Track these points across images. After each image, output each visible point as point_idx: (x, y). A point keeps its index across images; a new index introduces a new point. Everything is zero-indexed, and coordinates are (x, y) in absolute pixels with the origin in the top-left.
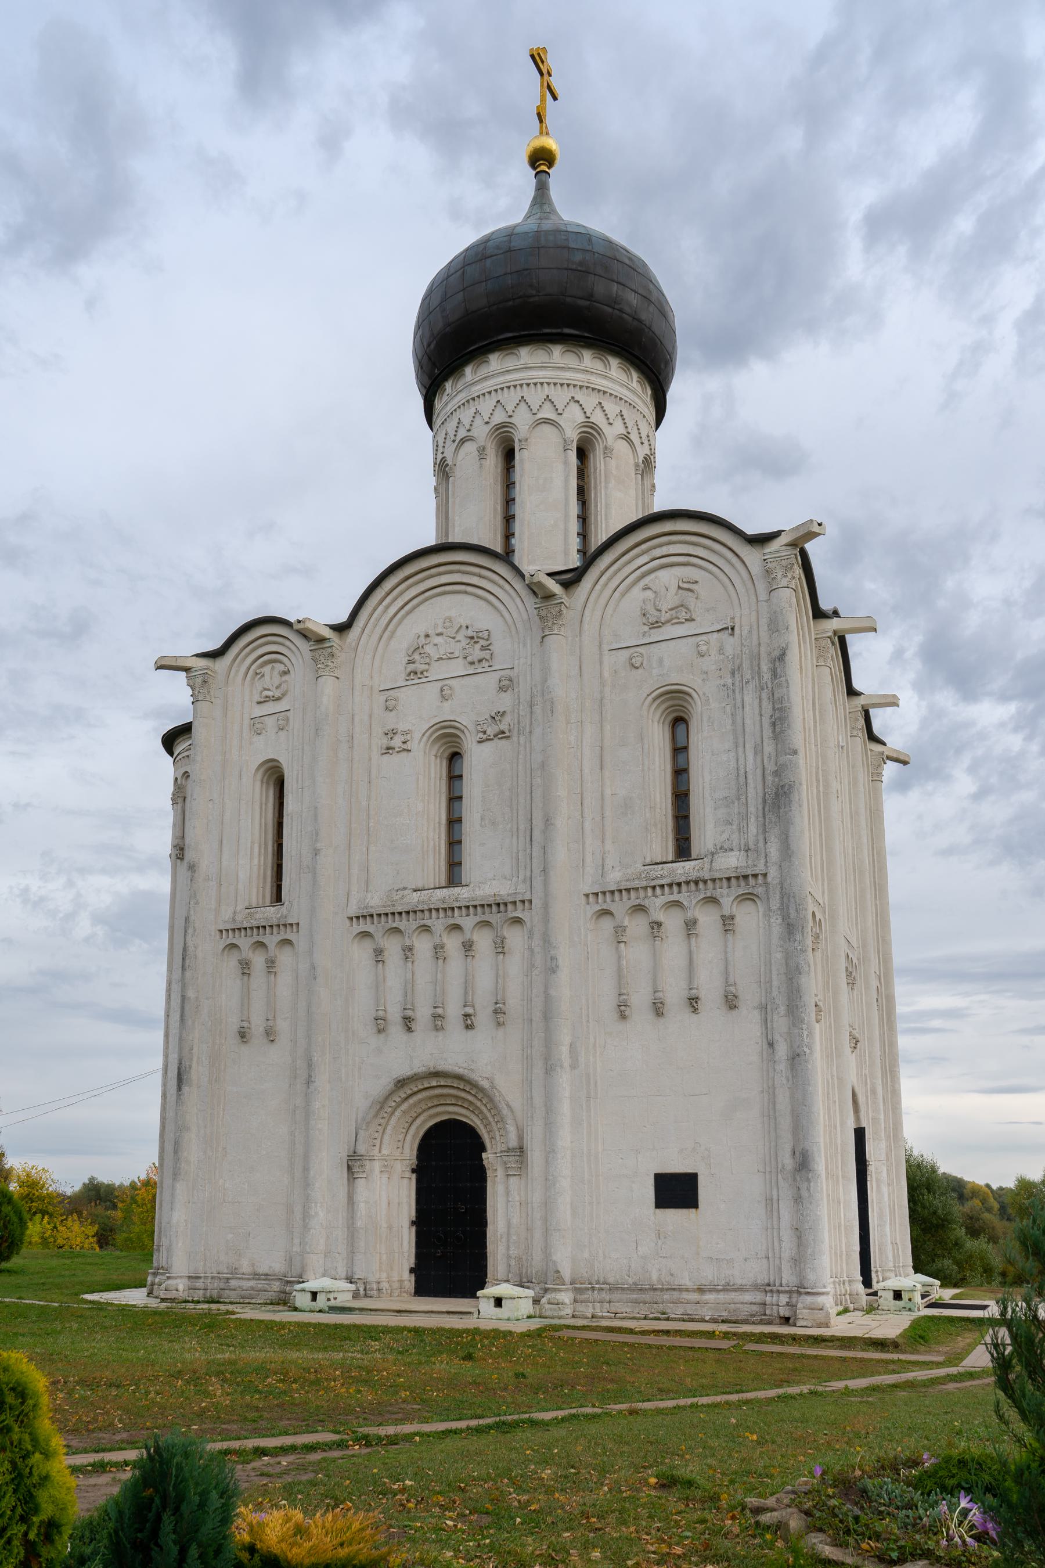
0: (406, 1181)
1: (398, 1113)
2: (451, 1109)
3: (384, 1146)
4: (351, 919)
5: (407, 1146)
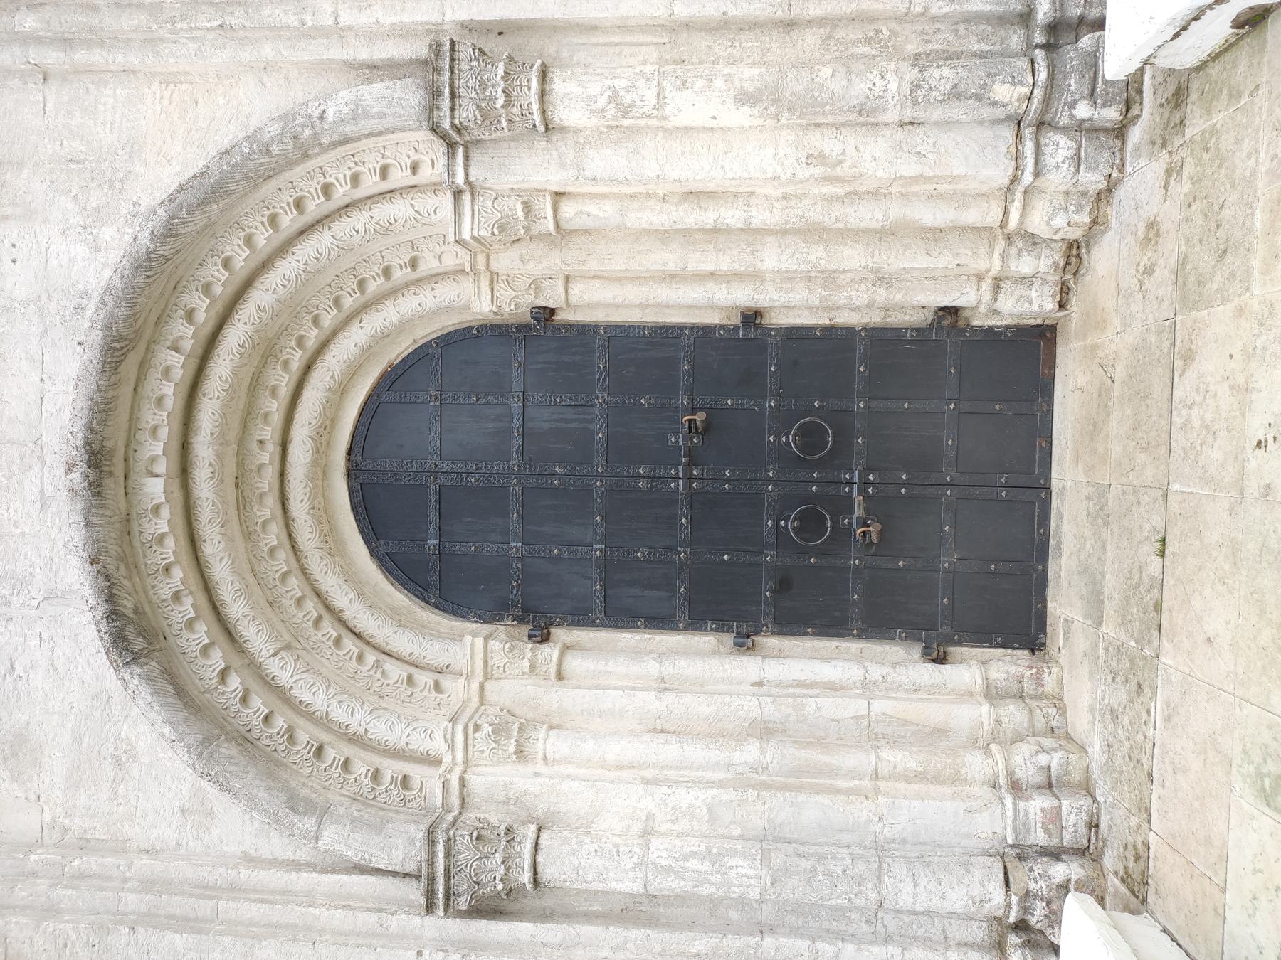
0: (575, 664)
1: (282, 671)
2: (300, 454)
3: (418, 743)
5: (435, 652)
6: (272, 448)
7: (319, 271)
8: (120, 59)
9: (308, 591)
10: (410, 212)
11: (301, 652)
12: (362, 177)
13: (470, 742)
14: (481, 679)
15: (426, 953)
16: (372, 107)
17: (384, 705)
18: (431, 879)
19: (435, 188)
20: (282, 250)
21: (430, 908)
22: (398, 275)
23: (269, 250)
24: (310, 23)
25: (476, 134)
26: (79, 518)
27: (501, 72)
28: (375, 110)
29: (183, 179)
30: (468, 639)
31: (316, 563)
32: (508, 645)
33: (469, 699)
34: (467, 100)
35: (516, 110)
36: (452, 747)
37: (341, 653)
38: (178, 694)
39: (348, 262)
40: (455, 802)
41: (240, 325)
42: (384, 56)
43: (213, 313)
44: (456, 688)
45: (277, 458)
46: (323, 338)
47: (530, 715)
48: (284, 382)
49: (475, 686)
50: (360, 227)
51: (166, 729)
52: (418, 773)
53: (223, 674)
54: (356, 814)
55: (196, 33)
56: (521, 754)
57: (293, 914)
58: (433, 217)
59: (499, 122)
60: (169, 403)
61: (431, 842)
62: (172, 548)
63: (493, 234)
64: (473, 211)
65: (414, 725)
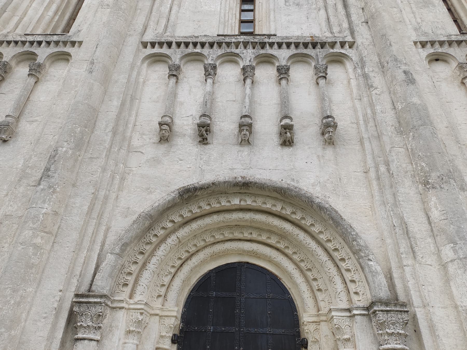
3: (139, 289)
4: (145, 45)
5: (172, 295)
6: (249, 237)
7: (313, 255)
8: (376, 194)
9: (198, 248)
10: (339, 290)
11: (177, 246)
12: (349, 273)
13: (137, 311)
14: (160, 315)
15: (60, 293)
16: (377, 278)
17: (155, 276)
18: (88, 296)
19: (350, 300)
20: (319, 243)
21: (77, 296)
22: (314, 284)
23: (319, 239)
24: (402, 256)
25: (374, 320)
26: (227, 180)
27: (400, 332)
28: (376, 280)
29: (339, 212)
30: (176, 309)
31: (208, 251)
32: (172, 326)
33: (153, 309)
34: (386, 317)
35: (386, 337)
36: (136, 303)
37: (176, 260)
38: (168, 208)
39: (317, 266)
40: (115, 305)
41: (292, 228)
42: (396, 283)
43: (295, 220)
44: (158, 304)
45: (246, 238)
46: (289, 255)
47: (143, 335)
48: (273, 241)
49: (158, 312)
50: (330, 271)
51: (157, 204)
52: (128, 290)
53: (173, 221)
54: (117, 267)
55: (390, 217)
56: (129, 332)
57: (86, 244)
58: (338, 299)
59: (380, 330)
60: (264, 206)
61: (101, 296)
62: (216, 206)
63: (335, 325)
64: (343, 317)
65: (146, 288)
